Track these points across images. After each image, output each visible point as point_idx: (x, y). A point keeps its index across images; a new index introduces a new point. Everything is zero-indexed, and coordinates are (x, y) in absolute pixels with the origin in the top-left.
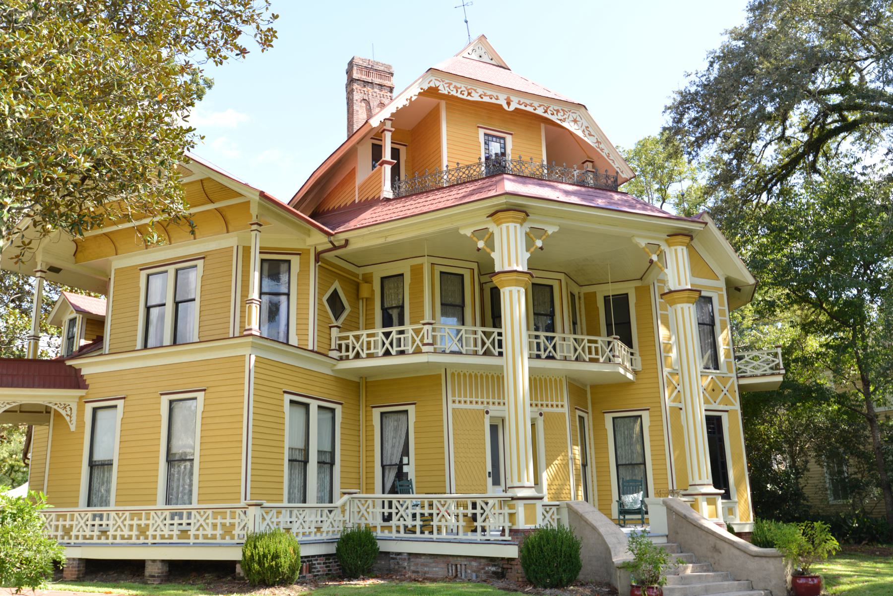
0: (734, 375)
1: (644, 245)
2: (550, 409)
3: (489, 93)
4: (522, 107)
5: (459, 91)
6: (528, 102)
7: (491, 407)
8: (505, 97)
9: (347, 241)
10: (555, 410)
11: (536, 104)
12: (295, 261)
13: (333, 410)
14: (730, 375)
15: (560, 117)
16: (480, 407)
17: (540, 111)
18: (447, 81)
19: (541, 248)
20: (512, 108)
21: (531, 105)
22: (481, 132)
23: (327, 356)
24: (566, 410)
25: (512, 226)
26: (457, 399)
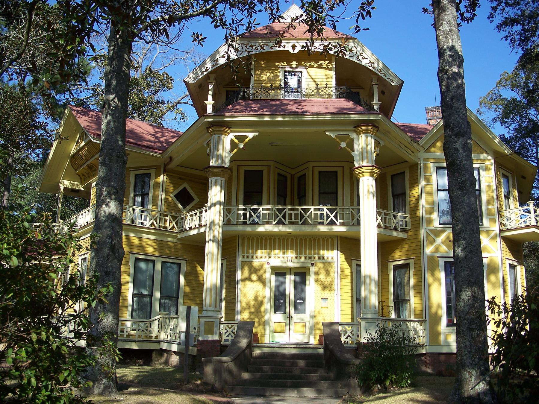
5: (254, 47)
8: (291, 44)
9: (171, 158)
13: (179, 265)
18: (244, 43)
20: (296, 51)
26: (246, 255)
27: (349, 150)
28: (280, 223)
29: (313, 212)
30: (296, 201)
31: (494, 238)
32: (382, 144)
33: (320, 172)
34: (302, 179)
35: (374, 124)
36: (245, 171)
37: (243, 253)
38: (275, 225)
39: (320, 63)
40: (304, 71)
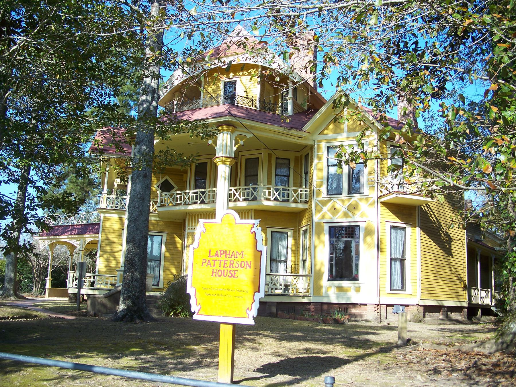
15: (255, 60)
26: (190, 227)
27: (214, 145)
28: (203, 202)
31: (372, 204)
33: (247, 160)
37: (189, 226)
38: (200, 203)
39: (250, 71)
40: (238, 79)
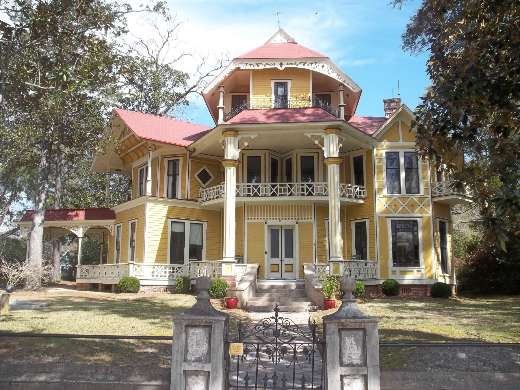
0: (430, 196)
1: (309, 136)
2: (303, 220)
3: (269, 63)
4: (290, 66)
6: (293, 63)
7: (269, 220)
10: (306, 220)
11: (298, 63)
12: (181, 159)
14: (426, 196)
16: (262, 220)
17: (301, 66)
19: (248, 146)
20: (284, 67)
21: (295, 64)
22: (273, 83)
23: (197, 201)
24: (313, 220)
25: (229, 138)
27: (320, 145)
28: (274, 195)
29: (297, 187)
30: (285, 177)
32: (344, 139)
33: (302, 157)
34: (289, 162)
35: (338, 128)
36: (248, 157)
